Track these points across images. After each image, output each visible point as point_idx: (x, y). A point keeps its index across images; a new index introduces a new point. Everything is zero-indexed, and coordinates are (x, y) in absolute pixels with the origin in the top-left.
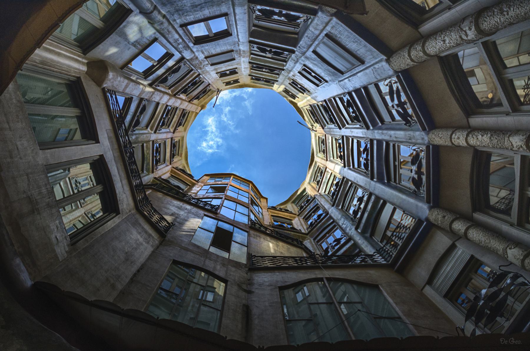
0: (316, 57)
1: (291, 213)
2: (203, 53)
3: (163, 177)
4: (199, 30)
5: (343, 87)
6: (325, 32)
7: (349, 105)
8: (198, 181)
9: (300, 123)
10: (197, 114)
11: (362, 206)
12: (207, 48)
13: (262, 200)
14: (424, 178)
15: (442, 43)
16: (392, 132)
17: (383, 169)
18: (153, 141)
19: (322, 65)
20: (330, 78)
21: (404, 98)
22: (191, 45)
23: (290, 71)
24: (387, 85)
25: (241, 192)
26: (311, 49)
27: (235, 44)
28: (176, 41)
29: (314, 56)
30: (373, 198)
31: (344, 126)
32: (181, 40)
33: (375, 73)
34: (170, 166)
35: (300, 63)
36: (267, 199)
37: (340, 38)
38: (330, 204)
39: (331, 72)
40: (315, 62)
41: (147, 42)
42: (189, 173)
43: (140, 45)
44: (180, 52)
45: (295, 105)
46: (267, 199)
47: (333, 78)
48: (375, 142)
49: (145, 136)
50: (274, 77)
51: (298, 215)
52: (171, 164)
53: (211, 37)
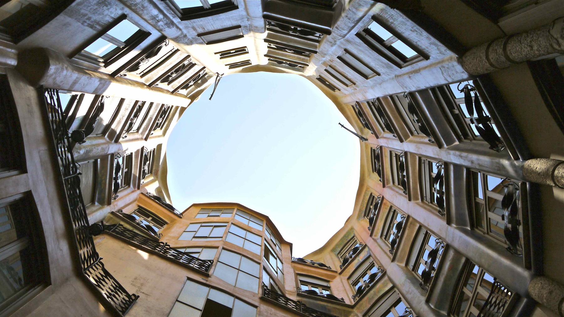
0: (361, 41)
1: (329, 269)
2: (194, 29)
3: (125, 211)
7: (414, 108)
8: (180, 216)
9: (342, 126)
10: (183, 109)
11: (436, 265)
12: (201, 23)
13: (283, 248)
14: (521, 229)
15: (529, 48)
16: (474, 157)
18: (112, 155)
19: (370, 53)
21: (486, 112)
22: (176, 20)
23: (325, 54)
25: (250, 236)
26: (354, 31)
27: (243, 19)
28: (154, 18)
29: (358, 40)
30: (451, 254)
32: (161, 16)
33: (445, 74)
34: (138, 192)
35: (339, 46)
36: (290, 245)
37: (392, 23)
38: (389, 257)
39: (385, 64)
41: (111, 20)
42: (168, 202)
43: (100, 25)
44: (160, 31)
46: (290, 245)
48: (452, 168)
49: (100, 148)
50: (303, 60)
51: (340, 274)
52: (139, 188)
53: (207, 9)
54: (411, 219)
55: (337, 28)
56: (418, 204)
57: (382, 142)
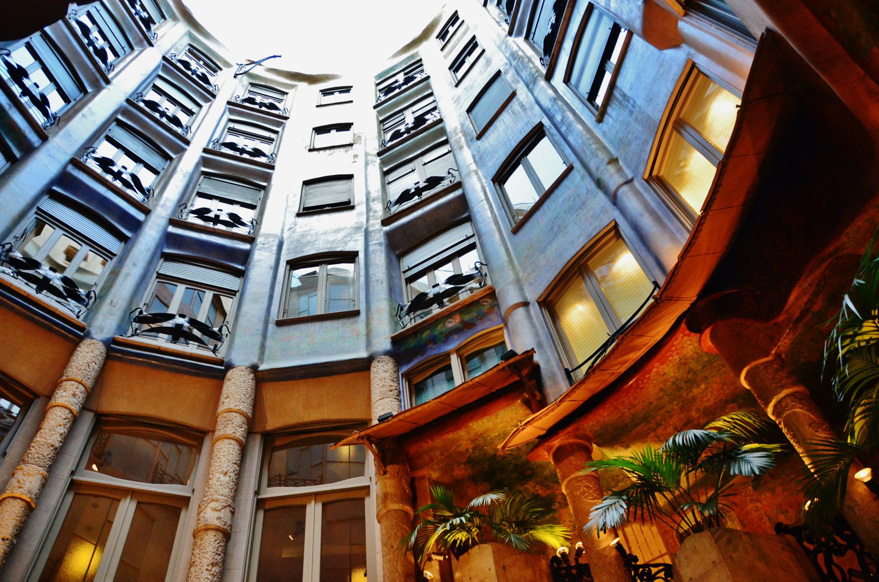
4: (546, 160)
5: (267, 236)
6: (363, 314)
9: (275, 57)
17: (79, 197)
19: (328, 242)
20: (299, 230)
24: (220, 330)
29: (350, 247)
31: (204, 162)
40: (340, 236)
45: (312, 79)
47: (295, 236)
54: (103, 83)
55: (380, 244)
56: (116, 112)
57: (219, 105)
